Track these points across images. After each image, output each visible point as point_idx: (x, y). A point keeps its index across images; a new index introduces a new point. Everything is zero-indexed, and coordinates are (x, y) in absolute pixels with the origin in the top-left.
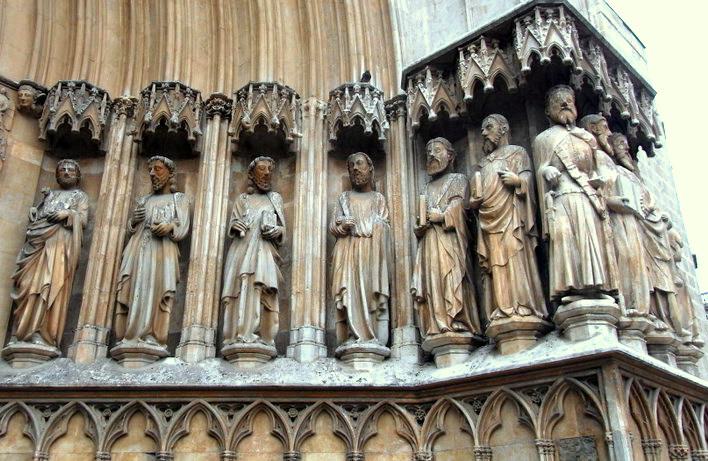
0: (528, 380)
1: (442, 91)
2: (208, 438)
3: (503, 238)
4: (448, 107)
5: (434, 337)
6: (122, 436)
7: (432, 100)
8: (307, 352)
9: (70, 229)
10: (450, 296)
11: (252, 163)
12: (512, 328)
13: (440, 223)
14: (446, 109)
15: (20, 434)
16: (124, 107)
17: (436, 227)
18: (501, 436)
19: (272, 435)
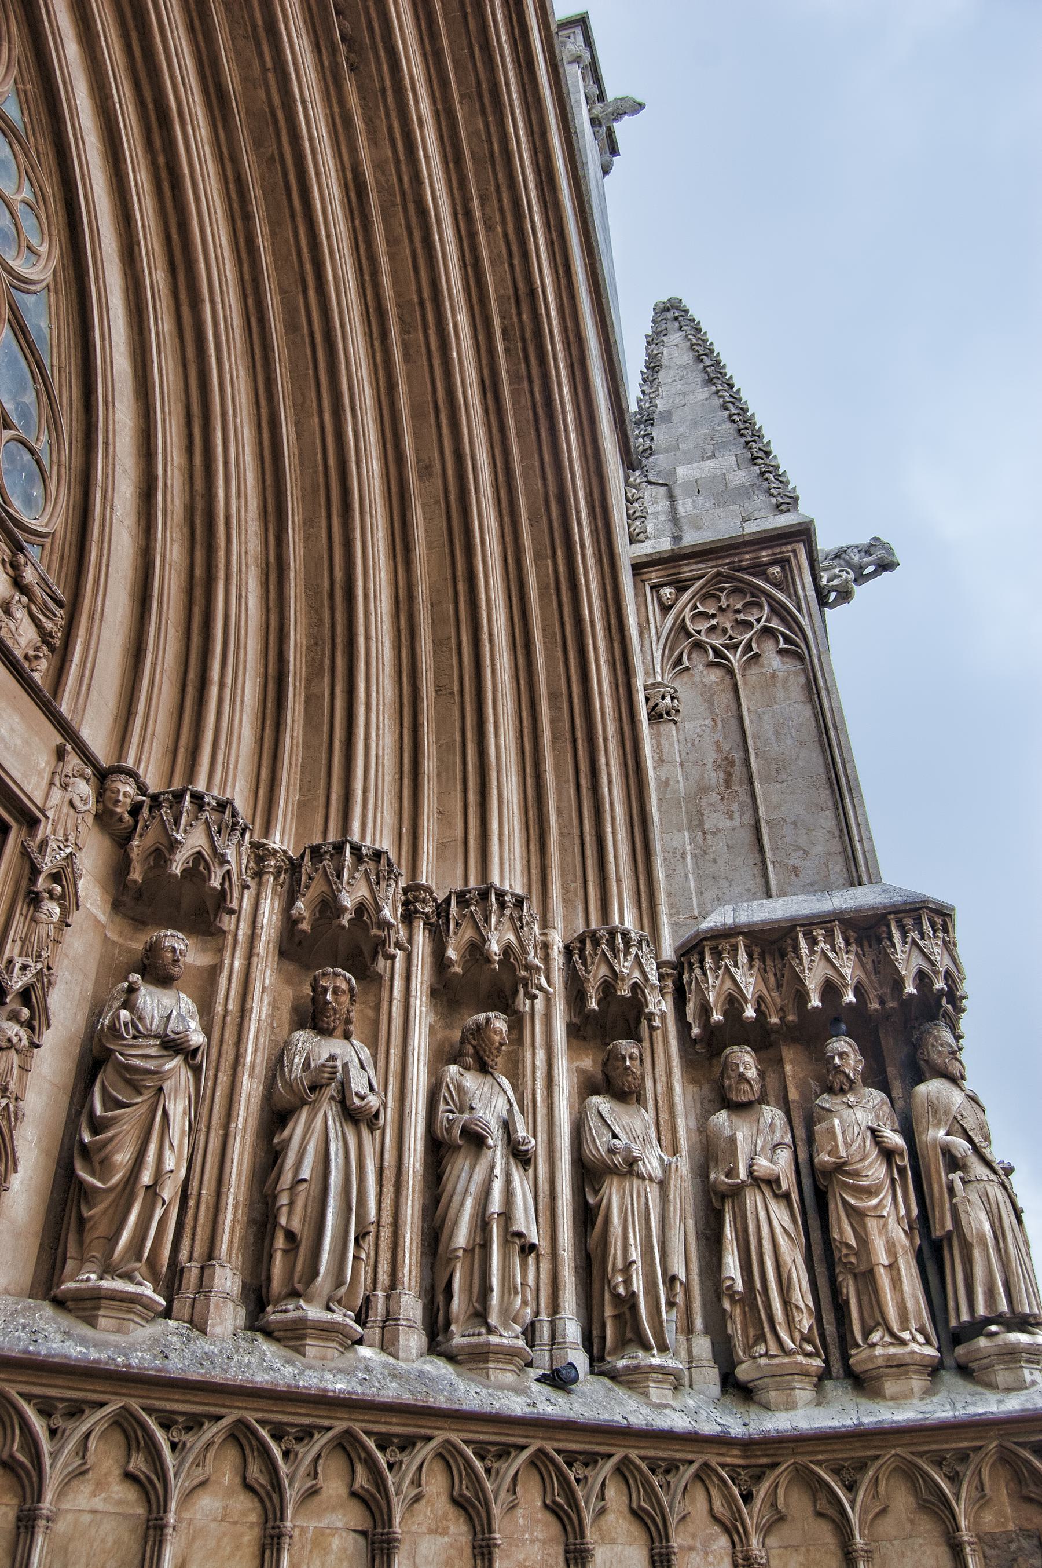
1: (760, 980)
2: (452, 1512)
3: (885, 1225)
5: (776, 1361)
7: (751, 989)
10: (797, 1297)
11: (481, 1017)
12: (908, 1360)
13: (772, 1183)
14: (763, 1007)
15: (117, 1472)
17: (763, 1186)
18: (887, 1526)
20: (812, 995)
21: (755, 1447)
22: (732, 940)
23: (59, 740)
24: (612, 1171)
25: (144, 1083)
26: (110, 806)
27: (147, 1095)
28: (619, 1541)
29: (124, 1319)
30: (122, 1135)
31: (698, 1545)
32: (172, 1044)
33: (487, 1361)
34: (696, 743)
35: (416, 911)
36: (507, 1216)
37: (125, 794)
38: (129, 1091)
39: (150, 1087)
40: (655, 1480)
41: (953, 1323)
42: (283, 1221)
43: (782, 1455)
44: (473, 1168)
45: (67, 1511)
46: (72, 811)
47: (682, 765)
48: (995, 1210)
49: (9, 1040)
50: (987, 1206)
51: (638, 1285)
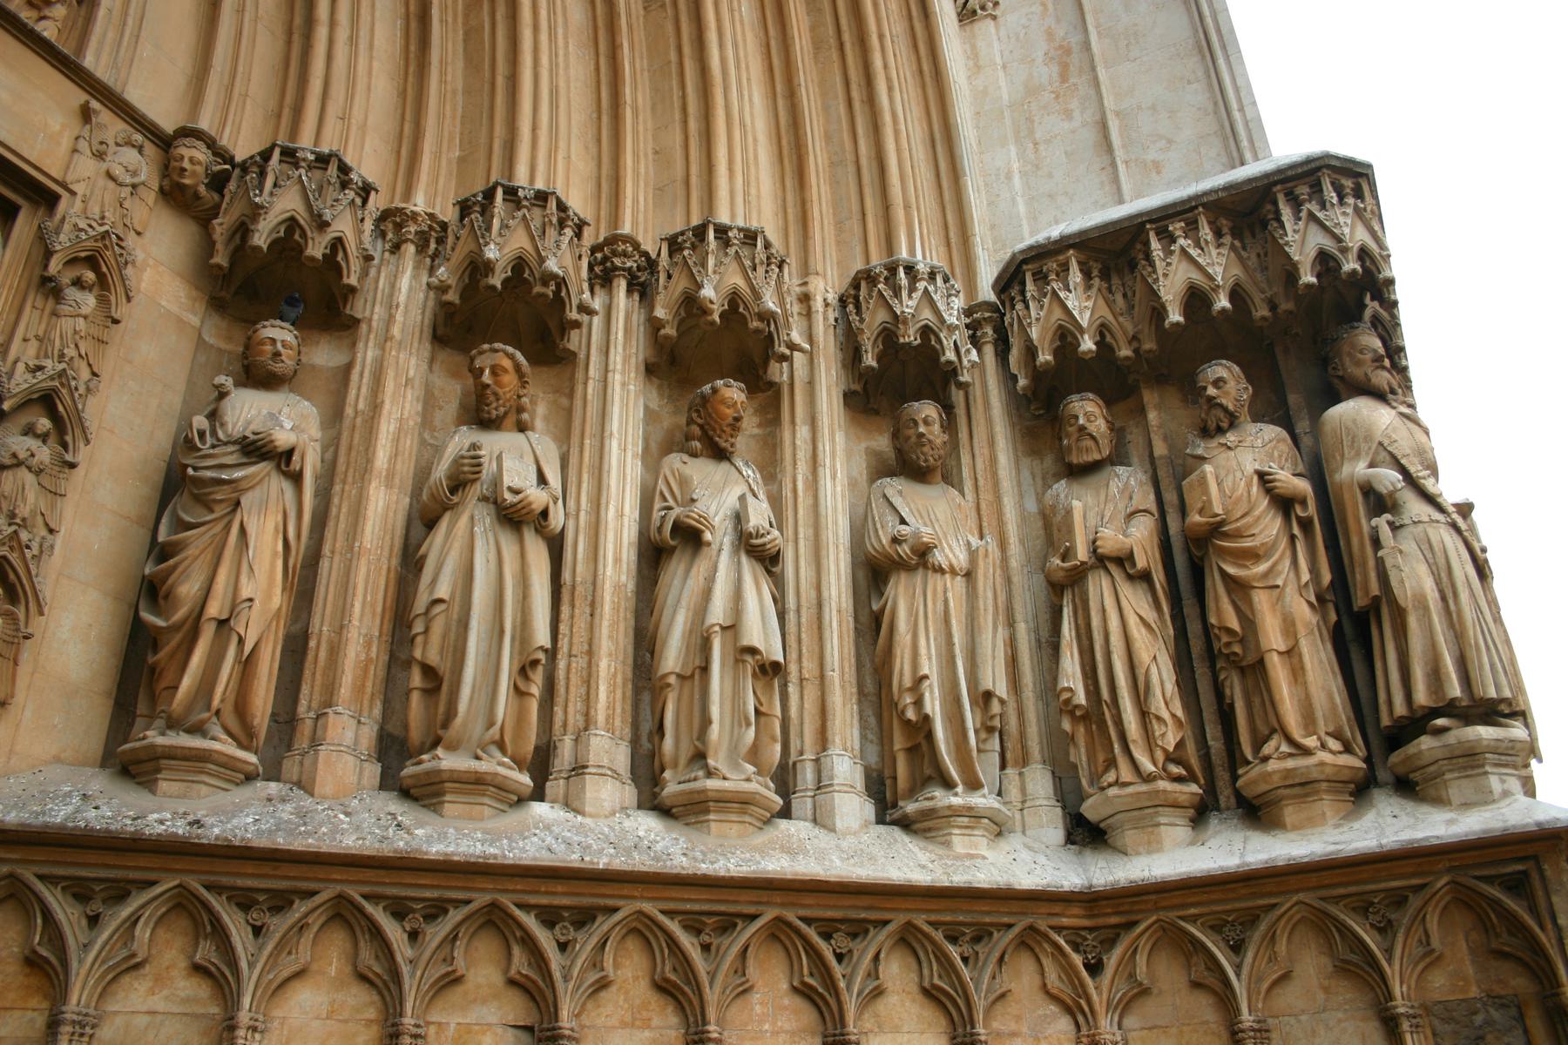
0: (1365, 882)
1: (1101, 302)
2: (654, 999)
3: (1280, 598)
4: (1113, 336)
5: (1130, 790)
6: (452, 980)
7: (1087, 314)
8: (852, 808)
9: (296, 478)
10: (1158, 705)
11: (707, 388)
12: (1315, 775)
13: (1123, 560)
14: (1108, 338)
15: (183, 964)
16: (413, 228)
17: (1109, 565)
18: (1290, 996)
19: (795, 990)
20: (1169, 309)
21: (1104, 902)
22: (1061, 258)
23: (79, 97)
24: (901, 565)
25: (213, 497)
26: (176, 177)
27: (220, 511)
28: (905, 1029)
29: (193, 782)
30: (186, 563)
31: (1025, 1030)
32: (252, 448)
33: (707, 811)
34: (1022, 35)
35: (616, 268)
36: (732, 629)
37: (191, 160)
38: (200, 510)
39: (221, 501)
40: (954, 952)
41: (1386, 721)
42: (418, 654)
43: (1140, 911)
44: (688, 571)
45: (116, 1013)
46: (111, 184)
47: (1004, 67)
48: (1442, 562)
49: (14, 455)
50: (1429, 556)
51: (934, 706)
